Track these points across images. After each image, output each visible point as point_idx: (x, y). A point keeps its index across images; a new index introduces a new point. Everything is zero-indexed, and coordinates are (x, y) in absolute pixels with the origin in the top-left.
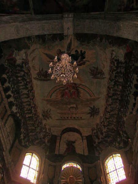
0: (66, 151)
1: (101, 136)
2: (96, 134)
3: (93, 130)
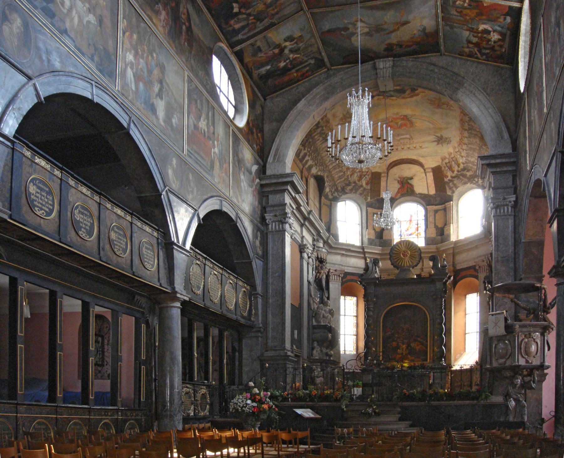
0: (398, 192)
1: (456, 168)
2: (448, 165)
3: (443, 159)
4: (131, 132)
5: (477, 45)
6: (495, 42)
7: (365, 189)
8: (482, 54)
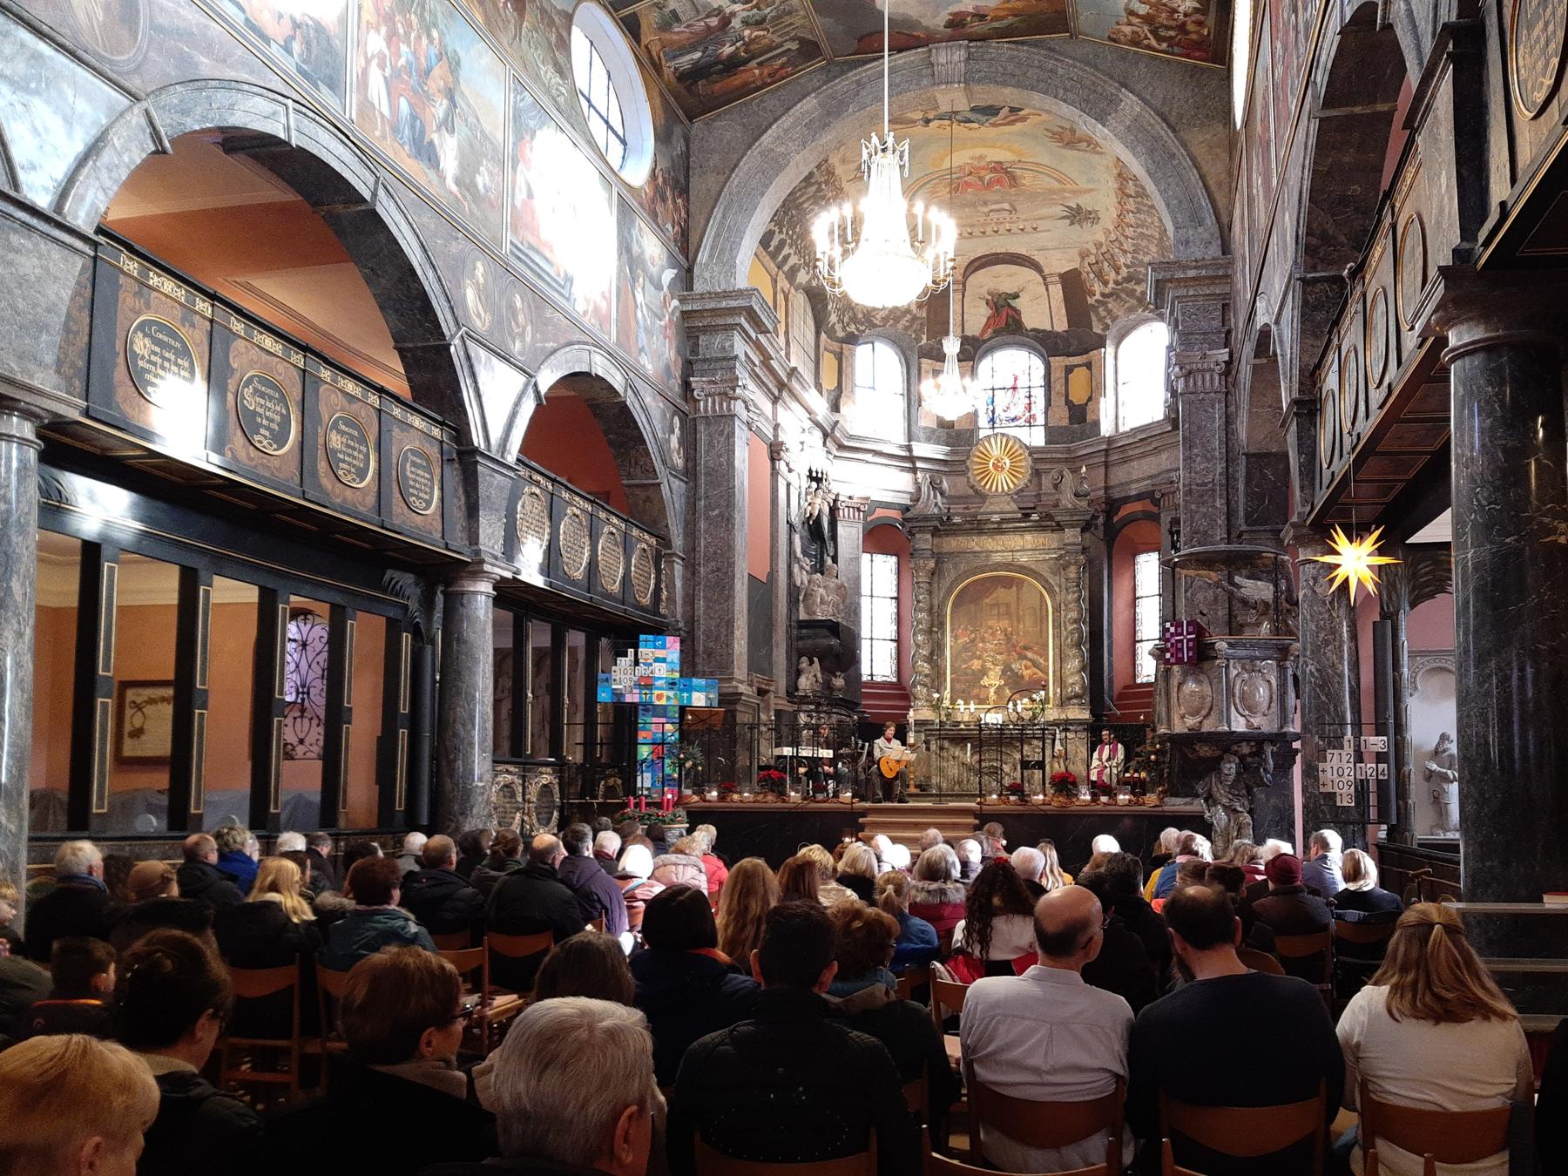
0: (987, 326)
1: (1112, 276)
3: (1083, 255)
4: (379, 210)
5: (1148, 19)
6: (1186, 15)
7: (915, 318)
8: (1160, 39)
